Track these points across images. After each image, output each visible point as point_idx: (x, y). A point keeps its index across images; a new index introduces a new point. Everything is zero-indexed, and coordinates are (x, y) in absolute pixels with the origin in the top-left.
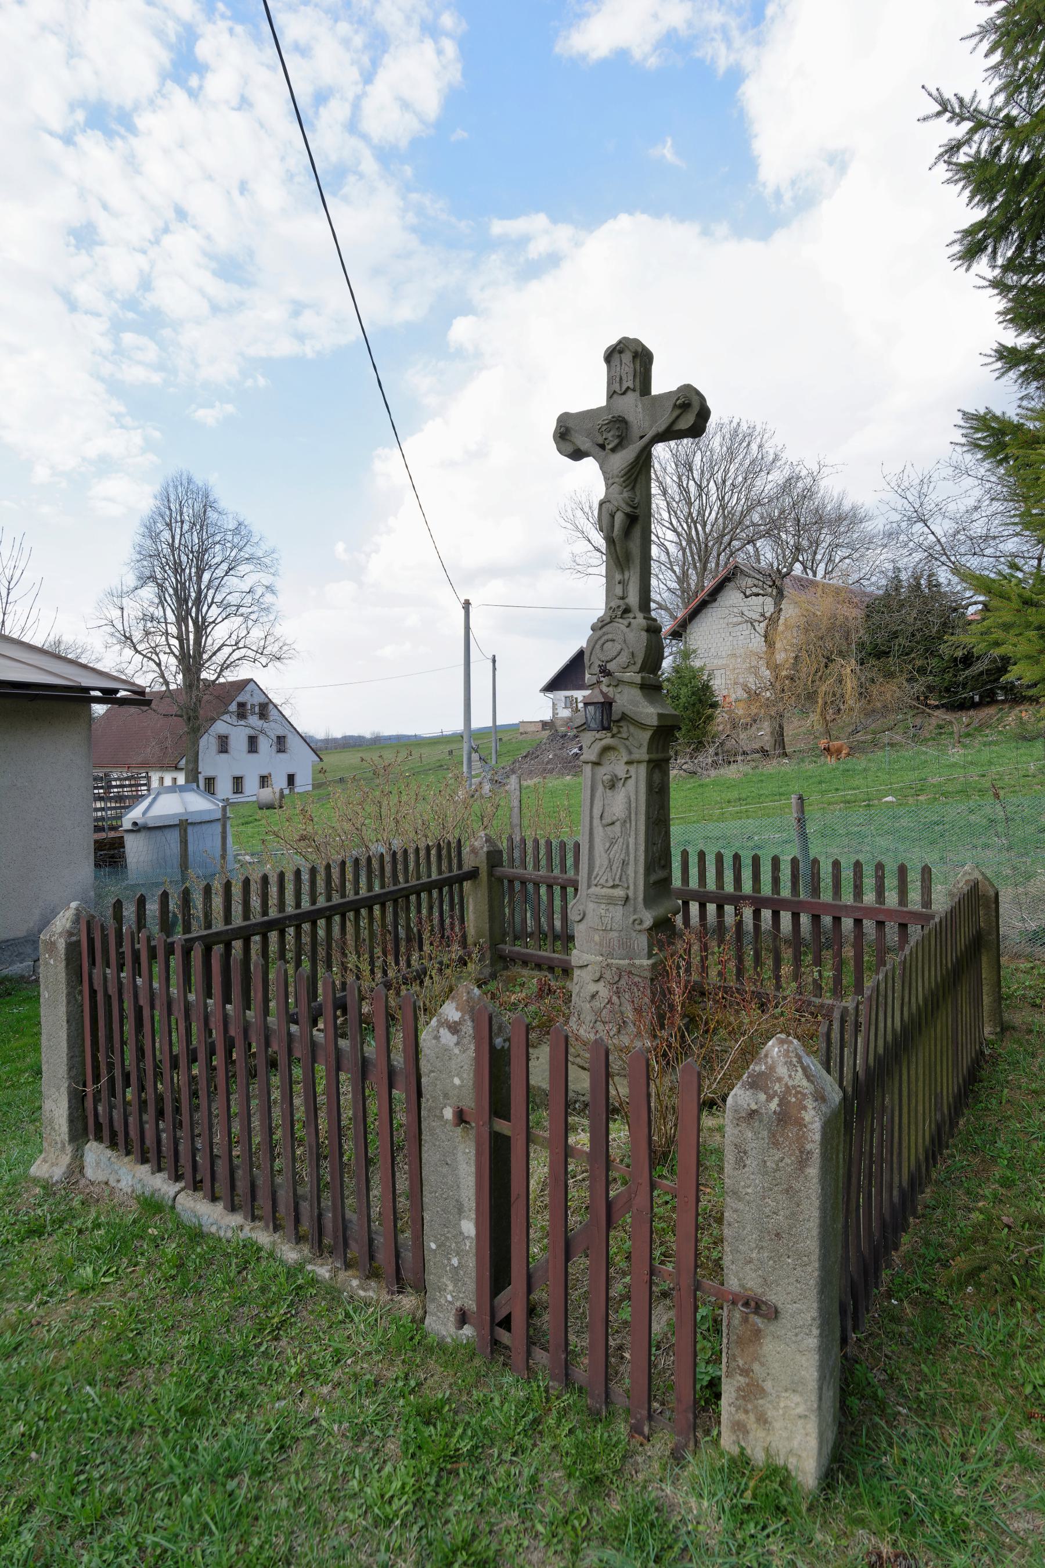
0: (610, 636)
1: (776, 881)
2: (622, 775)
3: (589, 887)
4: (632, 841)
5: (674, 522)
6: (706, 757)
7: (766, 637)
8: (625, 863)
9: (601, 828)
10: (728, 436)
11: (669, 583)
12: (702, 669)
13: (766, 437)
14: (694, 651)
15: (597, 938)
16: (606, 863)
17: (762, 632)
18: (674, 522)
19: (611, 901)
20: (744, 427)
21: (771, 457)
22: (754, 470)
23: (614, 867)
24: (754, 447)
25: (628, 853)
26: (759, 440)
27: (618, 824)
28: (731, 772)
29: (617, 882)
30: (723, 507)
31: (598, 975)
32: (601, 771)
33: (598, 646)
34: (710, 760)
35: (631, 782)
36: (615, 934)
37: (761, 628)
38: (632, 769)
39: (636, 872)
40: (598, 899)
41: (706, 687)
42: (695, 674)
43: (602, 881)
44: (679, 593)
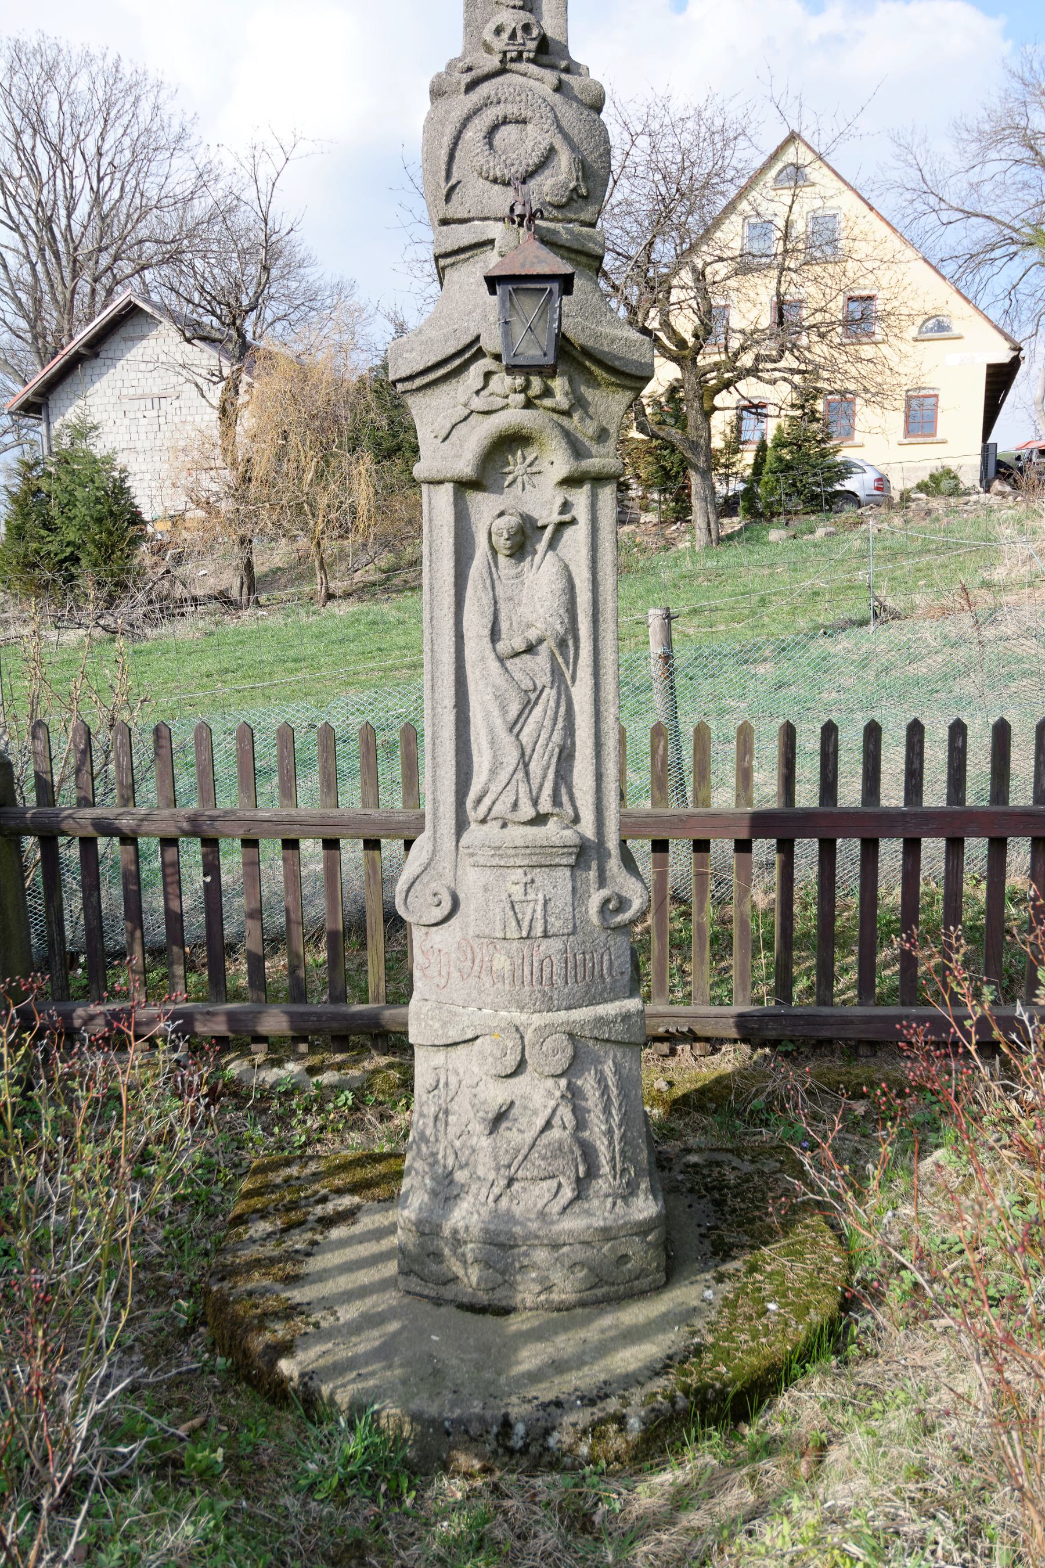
0: (511, 110)
1: (745, 776)
2: (548, 515)
3: (461, 825)
4: (581, 693)
5: (14, 212)
6: (130, 609)
7: (223, 411)
8: (566, 756)
9: (494, 665)
10: (100, 81)
11: (10, 318)
12: (109, 460)
13: (163, 95)
14: (95, 428)
15: (501, 962)
16: (511, 758)
17: (216, 402)
18: (14, 212)
19: (541, 859)
20: (126, 69)
21: (176, 129)
22: (144, 151)
23: (535, 767)
24: (145, 109)
25: (570, 729)
26: (151, 97)
27: (543, 649)
28: (184, 631)
29: (546, 805)
30: (98, 200)
31: (511, 1061)
32: (484, 508)
33: (474, 133)
34: (140, 611)
35: (577, 538)
36: (555, 945)
37: (216, 393)
38: (580, 497)
39: (599, 777)
40: (499, 861)
41: (120, 491)
42: (98, 465)
43: (500, 809)
44: (28, 336)
